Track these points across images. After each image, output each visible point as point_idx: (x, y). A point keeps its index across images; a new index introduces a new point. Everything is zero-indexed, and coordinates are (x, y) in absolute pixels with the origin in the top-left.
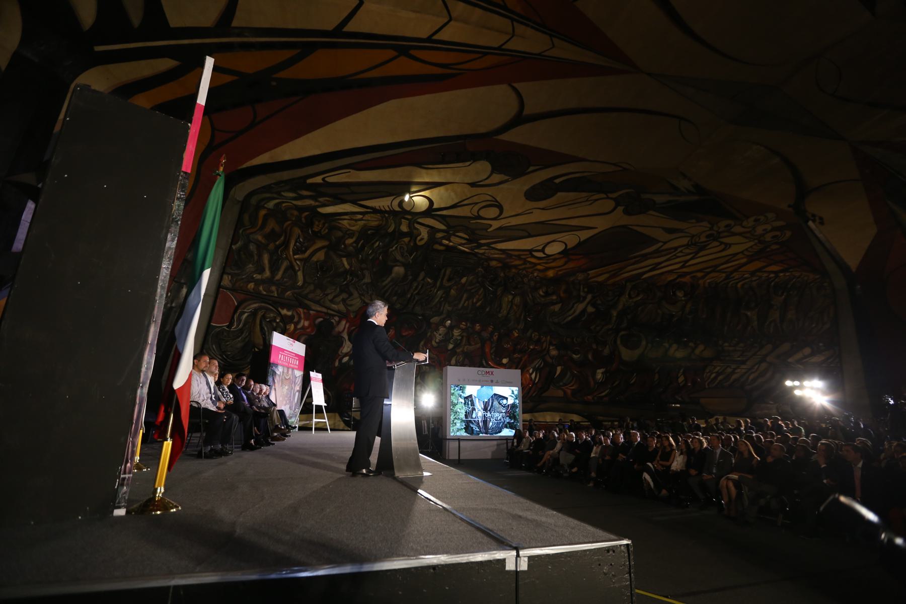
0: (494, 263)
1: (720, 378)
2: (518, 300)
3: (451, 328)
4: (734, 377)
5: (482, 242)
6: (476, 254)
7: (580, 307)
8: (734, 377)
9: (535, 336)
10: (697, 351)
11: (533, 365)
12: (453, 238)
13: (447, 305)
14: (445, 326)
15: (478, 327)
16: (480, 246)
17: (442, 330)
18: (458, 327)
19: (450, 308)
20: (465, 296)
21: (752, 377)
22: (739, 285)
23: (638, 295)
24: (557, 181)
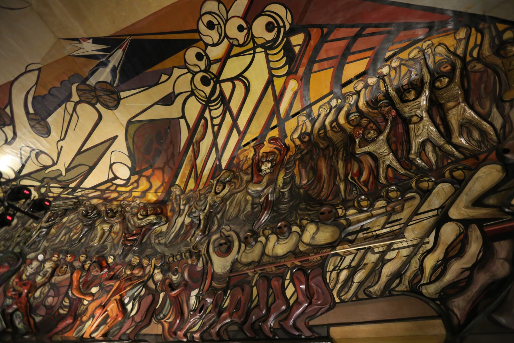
0: (95, 201)
1: (359, 277)
2: (117, 228)
3: (44, 261)
4: (388, 270)
5: (72, 185)
6: (77, 197)
7: (180, 220)
8: (388, 270)
9: (135, 260)
10: (307, 238)
11: (130, 293)
12: (52, 190)
13: (45, 242)
14: (38, 260)
15: (69, 258)
16: (74, 189)
17: (35, 264)
18: (50, 259)
19: (47, 245)
20: (63, 232)
21: (430, 262)
22: (342, 120)
23: (224, 188)
24: (31, 110)
